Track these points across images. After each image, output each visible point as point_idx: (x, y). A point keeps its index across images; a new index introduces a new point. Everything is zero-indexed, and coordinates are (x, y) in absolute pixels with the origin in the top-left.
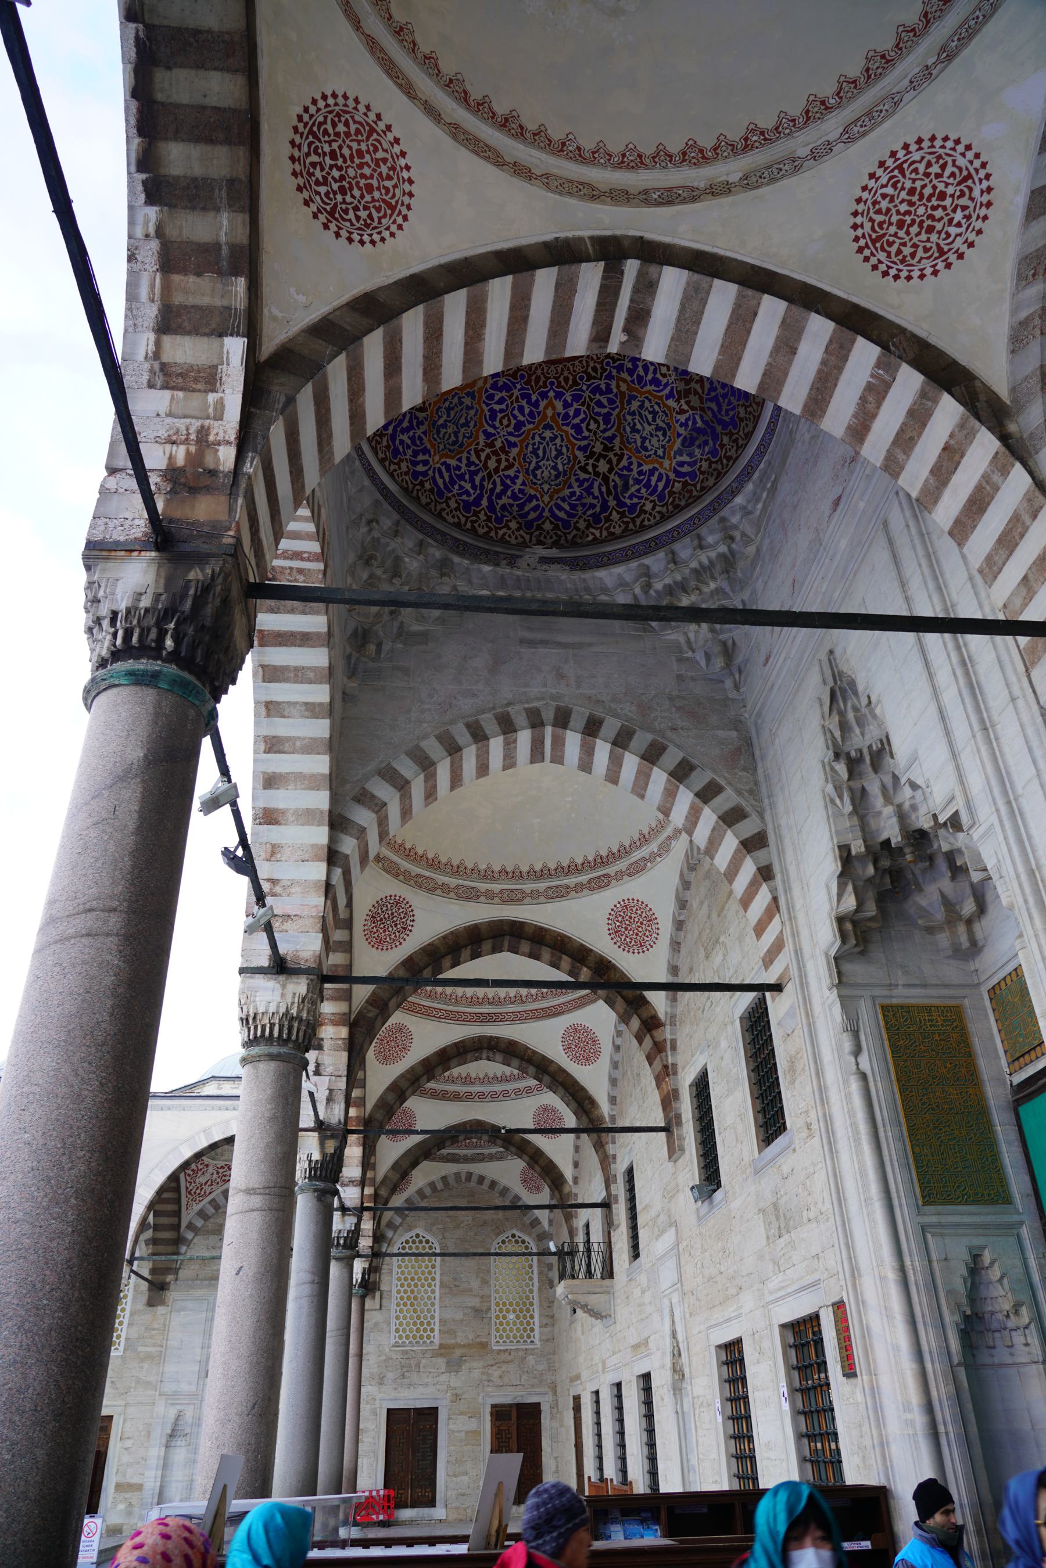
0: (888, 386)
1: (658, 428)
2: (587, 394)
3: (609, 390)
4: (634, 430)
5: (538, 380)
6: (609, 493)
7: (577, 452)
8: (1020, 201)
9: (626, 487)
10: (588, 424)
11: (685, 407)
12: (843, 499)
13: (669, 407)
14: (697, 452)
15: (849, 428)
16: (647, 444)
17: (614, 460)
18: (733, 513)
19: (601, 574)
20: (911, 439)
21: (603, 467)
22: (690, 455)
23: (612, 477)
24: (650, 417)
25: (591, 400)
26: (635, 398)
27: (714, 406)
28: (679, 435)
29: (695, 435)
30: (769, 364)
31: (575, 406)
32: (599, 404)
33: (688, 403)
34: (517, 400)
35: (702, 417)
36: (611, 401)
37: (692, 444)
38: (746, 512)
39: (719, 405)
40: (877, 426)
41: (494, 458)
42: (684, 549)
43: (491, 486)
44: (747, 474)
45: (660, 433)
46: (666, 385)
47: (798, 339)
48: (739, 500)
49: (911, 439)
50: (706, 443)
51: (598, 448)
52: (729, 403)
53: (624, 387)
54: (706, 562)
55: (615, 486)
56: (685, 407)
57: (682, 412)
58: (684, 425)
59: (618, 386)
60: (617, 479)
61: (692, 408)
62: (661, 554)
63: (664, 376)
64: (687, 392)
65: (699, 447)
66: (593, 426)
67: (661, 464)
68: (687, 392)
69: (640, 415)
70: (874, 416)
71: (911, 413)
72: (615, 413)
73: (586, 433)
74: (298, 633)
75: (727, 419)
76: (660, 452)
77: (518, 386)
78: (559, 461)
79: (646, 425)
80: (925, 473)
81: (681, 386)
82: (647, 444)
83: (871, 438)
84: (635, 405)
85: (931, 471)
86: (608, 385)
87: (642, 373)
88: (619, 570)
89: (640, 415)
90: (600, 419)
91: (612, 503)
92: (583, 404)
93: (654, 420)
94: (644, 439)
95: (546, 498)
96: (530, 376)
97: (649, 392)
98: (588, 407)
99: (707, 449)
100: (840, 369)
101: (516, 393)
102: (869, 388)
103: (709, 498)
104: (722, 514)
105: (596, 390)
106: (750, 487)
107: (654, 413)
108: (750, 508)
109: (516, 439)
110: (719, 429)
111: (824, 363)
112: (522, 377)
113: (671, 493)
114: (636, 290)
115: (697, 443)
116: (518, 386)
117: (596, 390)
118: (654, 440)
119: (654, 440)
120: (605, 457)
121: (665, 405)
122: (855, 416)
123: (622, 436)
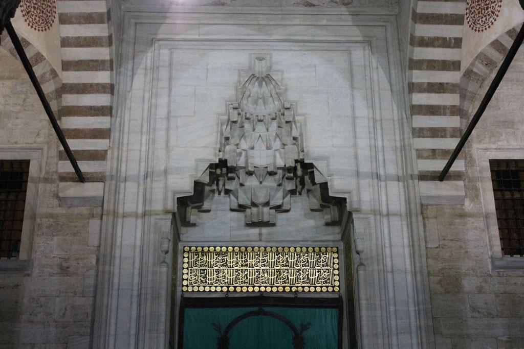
0: (449, 47)
8: (494, 38)
12: (312, 9)
15: (423, 38)
20: (434, 67)
40: (430, 50)
49: (434, 67)
70: (434, 47)
71: (444, 62)
80: (426, 80)
83: (424, 49)
85: (429, 83)
100: (446, 23)
102: (444, 39)
111: (446, 15)
122: (429, 38)
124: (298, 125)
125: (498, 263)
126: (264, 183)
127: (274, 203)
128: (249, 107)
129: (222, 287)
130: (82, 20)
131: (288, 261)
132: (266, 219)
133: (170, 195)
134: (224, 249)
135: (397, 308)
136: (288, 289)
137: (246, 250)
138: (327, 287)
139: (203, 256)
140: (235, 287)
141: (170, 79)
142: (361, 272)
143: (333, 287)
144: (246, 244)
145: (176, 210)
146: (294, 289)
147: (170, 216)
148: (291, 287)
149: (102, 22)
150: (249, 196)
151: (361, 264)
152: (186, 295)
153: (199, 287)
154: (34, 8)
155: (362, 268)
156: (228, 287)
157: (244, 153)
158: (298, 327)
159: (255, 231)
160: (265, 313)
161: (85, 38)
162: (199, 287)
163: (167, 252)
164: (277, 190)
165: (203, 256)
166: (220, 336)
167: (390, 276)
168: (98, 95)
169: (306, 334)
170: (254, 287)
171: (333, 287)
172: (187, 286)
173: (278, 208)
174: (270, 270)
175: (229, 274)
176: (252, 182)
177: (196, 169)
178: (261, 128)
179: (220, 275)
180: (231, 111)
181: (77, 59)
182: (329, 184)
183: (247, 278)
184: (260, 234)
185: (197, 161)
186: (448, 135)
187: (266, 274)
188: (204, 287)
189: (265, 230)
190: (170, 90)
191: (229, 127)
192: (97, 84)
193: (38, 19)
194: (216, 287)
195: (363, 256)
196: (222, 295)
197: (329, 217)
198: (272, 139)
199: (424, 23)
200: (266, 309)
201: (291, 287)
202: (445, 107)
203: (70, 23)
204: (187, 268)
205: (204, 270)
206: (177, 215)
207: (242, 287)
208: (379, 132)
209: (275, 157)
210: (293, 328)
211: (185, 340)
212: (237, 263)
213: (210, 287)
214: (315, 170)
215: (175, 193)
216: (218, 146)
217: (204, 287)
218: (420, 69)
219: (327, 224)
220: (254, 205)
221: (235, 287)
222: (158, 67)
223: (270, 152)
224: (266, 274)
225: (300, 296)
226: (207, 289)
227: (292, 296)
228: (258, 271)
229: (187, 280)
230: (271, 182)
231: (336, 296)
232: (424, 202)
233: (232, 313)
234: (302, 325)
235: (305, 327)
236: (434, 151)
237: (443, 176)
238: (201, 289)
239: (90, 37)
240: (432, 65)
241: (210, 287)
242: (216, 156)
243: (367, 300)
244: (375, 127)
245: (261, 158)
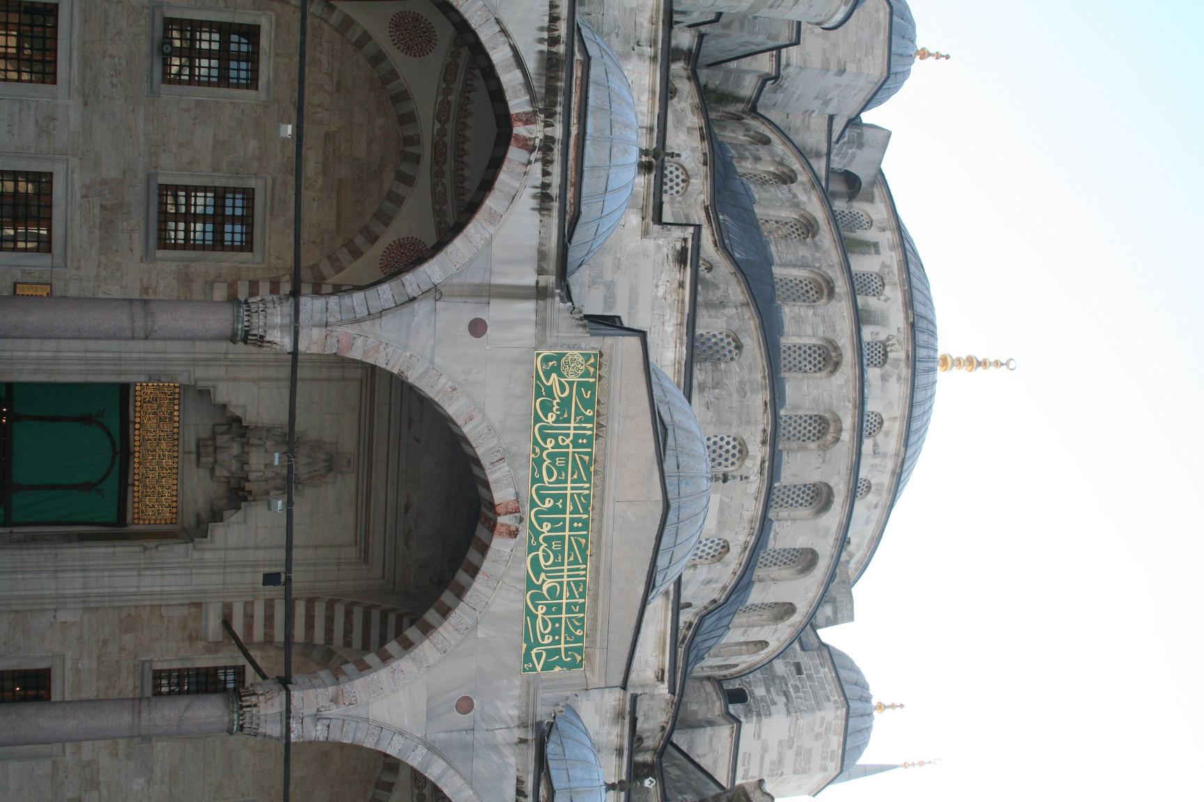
40: (342, 620)
83: (342, 614)
102: (351, 632)
125: (147, 666)
132: (203, 460)
133: (212, 383)
134: (176, 419)
136: (136, 477)
141: (329, 380)
142: (138, 549)
151: (146, 549)
158: (99, 487)
159: (193, 448)
160: (113, 458)
167: (135, 573)
173: (212, 470)
175: (151, 423)
177: (236, 406)
184: (190, 453)
185: (245, 407)
189: (193, 456)
195: (154, 551)
196: (131, 418)
215: (214, 387)
219: (198, 515)
220: (216, 448)
223: (262, 467)
225: (130, 489)
226: (138, 404)
227: (130, 481)
230: (235, 466)
232: (204, 607)
233: (115, 430)
236: (252, 617)
238: (138, 398)
245: (256, 460)
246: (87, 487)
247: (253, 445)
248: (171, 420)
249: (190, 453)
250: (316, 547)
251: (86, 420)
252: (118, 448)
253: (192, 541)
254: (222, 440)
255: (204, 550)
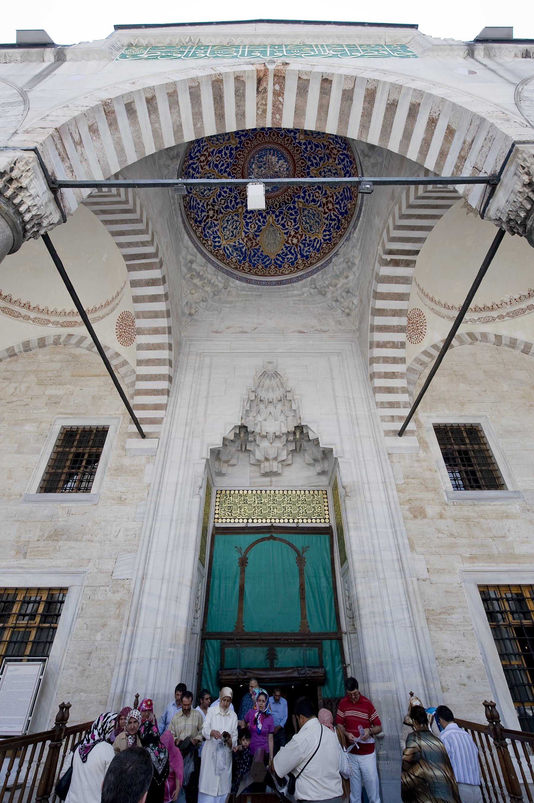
0: (397, 348)
1: (232, 232)
2: (233, 194)
3: (237, 204)
4: (228, 221)
5: (235, 169)
6: (205, 221)
7: (212, 199)
8: (423, 349)
9: (210, 228)
10: (223, 199)
11: (245, 241)
12: (303, 334)
13: (241, 234)
14: (235, 254)
15: (379, 342)
16: (226, 229)
17: (215, 218)
18: (233, 283)
19: (186, 237)
20: (388, 361)
21: (211, 213)
22: (232, 251)
23: (210, 219)
24: (234, 227)
25: (231, 197)
26: (238, 217)
27: (253, 254)
28: (235, 242)
29: (239, 249)
30: (387, 310)
31: (228, 190)
32: (231, 201)
33: (247, 241)
34: (226, 162)
35: (246, 250)
36: (233, 206)
37: (236, 250)
38: (236, 287)
39: (254, 256)
41: (204, 158)
42: (210, 268)
43: (195, 161)
44: (248, 281)
45: (231, 234)
46: (248, 229)
47: (397, 316)
48: (238, 282)
49: (388, 361)
50: (240, 257)
51: (216, 208)
52: (258, 260)
53: (240, 210)
54: (212, 282)
55: (208, 223)
56: (245, 241)
57: (243, 240)
58: (240, 244)
59: (240, 208)
60: (210, 222)
61: (246, 244)
62: (204, 260)
63: (251, 227)
64: (250, 239)
65: (237, 254)
66: (223, 201)
67: (223, 240)
68: (250, 239)
69: (233, 222)
70: (387, 348)
72: (230, 210)
73: (219, 199)
74: (224, 112)
75: (253, 261)
76: (226, 237)
77: (232, 161)
78: (207, 191)
79: (231, 226)
80: (383, 371)
81: (251, 236)
82: (226, 229)
83: (380, 349)
84: (236, 218)
86: (239, 203)
87: (248, 217)
88: (190, 244)
89: (233, 222)
90: (226, 204)
91: (203, 224)
92: (229, 194)
93: (234, 229)
94: (226, 227)
95: (194, 192)
96: (236, 165)
97: (243, 222)
98: (229, 197)
99: (238, 257)
101: (229, 160)
102: (394, 342)
103: (228, 268)
104: (230, 278)
105: (236, 198)
106: (245, 284)
107: (236, 228)
108: (239, 288)
109: (211, 167)
110: (247, 259)
111: (394, 326)
112: (236, 162)
113: (218, 250)
114: (406, 260)
115: (237, 252)
116: (232, 161)
117: (236, 198)
118: (228, 232)
119: (228, 232)
120: (214, 212)
121: (241, 232)
122: (384, 342)
123: (223, 217)
124: (296, 401)
125: (451, 496)
126: (274, 444)
127: (280, 458)
128: (263, 394)
129: (243, 519)
130: (151, 332)
131: (291, 500)
132: (275, 470)
133: (205, 447)
135: (378, 530)
137: (261, 493)
138: (320, 519)
139: (230, 496)
140: (253, 519)
142: (347, 502)
143: (325, 519)
144: (261, 488)
145: (209, 458)
146: (296, 521)
147: (205, 461)
148: (294, 519)
149: (164, 333)
150: (263, 453)
152: (217, 525)
153: (226, 519)
154: (124, 332)
155: (347, 498)
156: (248, 519)
157: (259, 424)
159: (267, 479)
160: (275, 539)
161: (153, 344)
162: (226, 519)
163: (201, 488)
164: (283, 449)
165: (230, 496)
166: (241, 556)
167: (369, 505)
168: (160, 382)
169: (305, 555)
170: (266, 519)
171: (325, 519)
172: (218, 519)
174: (278, 507)
176: (265, 444)
178: (271, 408)
179: (242, 510)
180: (251, 393)
181: (147, 358)
182: (319, 439)
183: (262, 513)
184: (271, 481)
186: (401, 406)
187: (275, 510)
188: (230, 519)
189: (274, 479)
190: (209, 380)
191: (249, 403)
192: (160, 375)
193: (126, 339)
194: (239, 519)
197: (320, 468)
198: (279, 413)
199: (379, 332)
200: (275, 535)
201: (294, 519)
202: (397, 388)
203: (144, 334)
204: (219, 506)
205: (230, 507)
206: (210, 461)
207: (257, 519)
208: (352, 406)
209: (281, 426)
210: (296, 550)
211: (214, 559)
212: (255, 502)
213: (235, 519)
214: (309, 430)
216: (241, 414)
217: (230, 519)
218: (378, 363)
219: (319, 474)
221: (253, 519)
222: (202, 368)
224: (275, 510)
228: (269, 507)
229: (218, 514)
230: (278, 444)
231: (327, 525)
232: (390, 452)
234: (303, 548)
235: (305, 549)
236: (393, 417)
237: (401, 433)
239: (156, 344)
240: (386, 360)
241: (235, 519)
242: (239, 421)
243: (354, 523)
244: (349, 403)
246: (301, 560)
247: (261, 430)
248: (246, 496)
249: (271, 481)
250: (332, 379)
251: (243, 562)
252: (268, 535)
253: (336, 459)
254: (259, 455)
255: (343, 450)
